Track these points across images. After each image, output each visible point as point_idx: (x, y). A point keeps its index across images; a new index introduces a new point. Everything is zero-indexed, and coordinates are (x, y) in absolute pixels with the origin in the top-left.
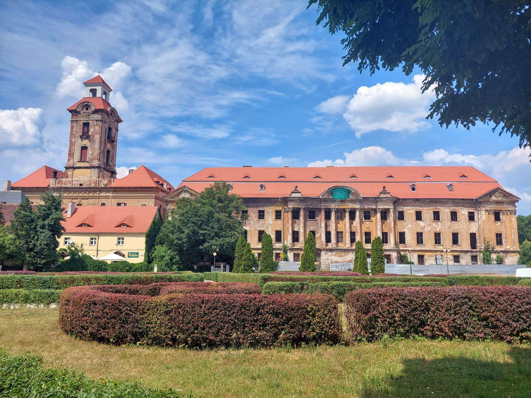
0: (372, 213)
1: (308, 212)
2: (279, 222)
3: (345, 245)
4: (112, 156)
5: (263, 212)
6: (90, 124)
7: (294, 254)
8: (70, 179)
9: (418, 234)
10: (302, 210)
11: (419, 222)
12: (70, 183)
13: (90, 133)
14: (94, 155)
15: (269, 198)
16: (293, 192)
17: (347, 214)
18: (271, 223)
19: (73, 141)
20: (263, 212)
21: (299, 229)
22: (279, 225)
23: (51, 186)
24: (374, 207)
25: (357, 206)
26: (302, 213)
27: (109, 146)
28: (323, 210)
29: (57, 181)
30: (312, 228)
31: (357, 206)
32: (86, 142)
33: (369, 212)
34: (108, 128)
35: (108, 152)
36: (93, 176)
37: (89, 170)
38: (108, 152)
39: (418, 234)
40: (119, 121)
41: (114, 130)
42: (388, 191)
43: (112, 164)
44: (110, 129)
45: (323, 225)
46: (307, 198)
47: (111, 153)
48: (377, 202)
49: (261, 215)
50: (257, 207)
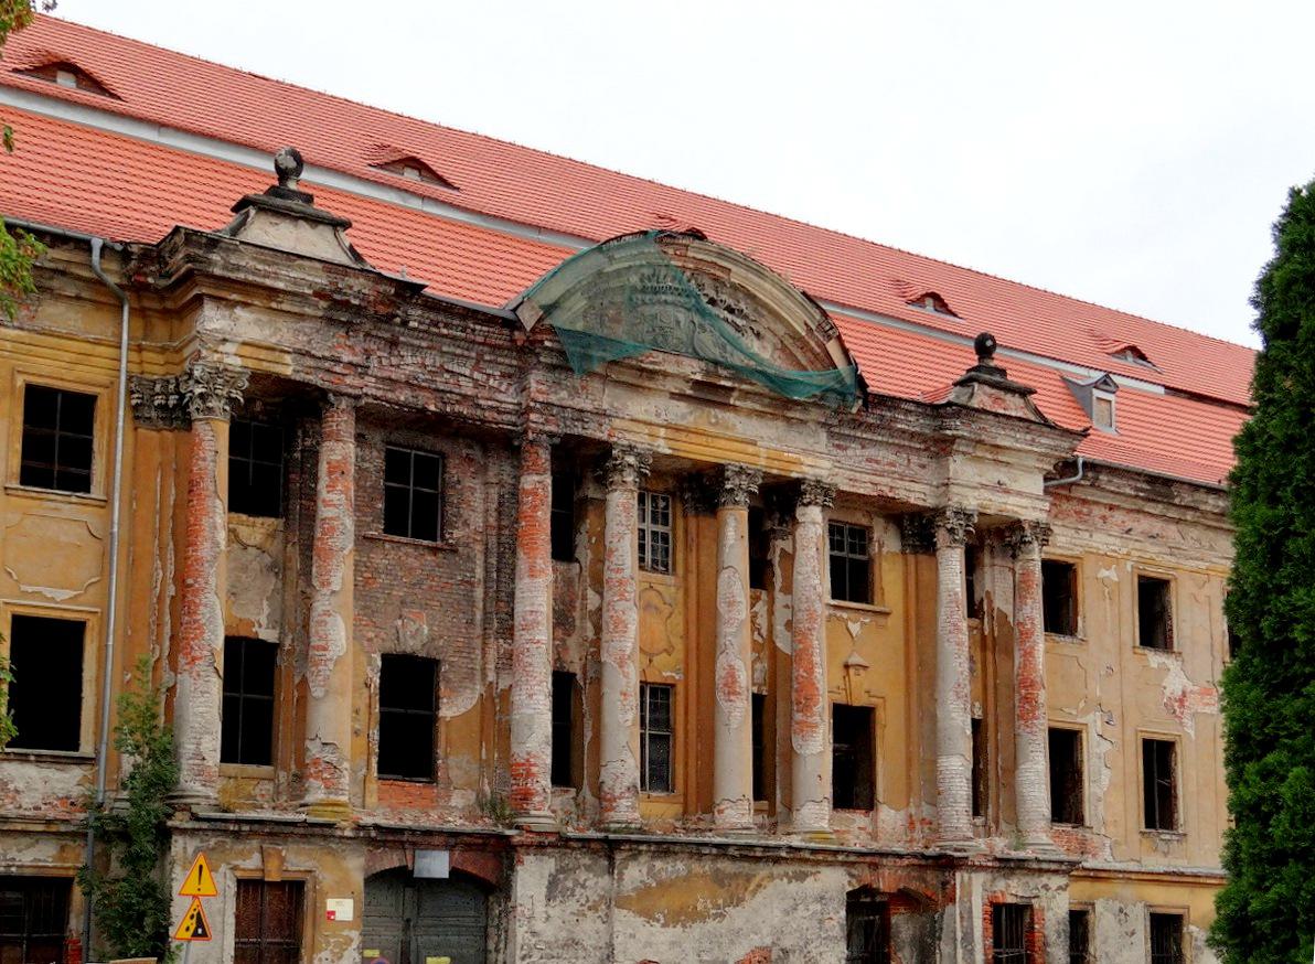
0: (886, 543)
2: (59, 513)
3: (704, 799)
7: (249, 888)
9: (1148, 745)
10: (341, 422)
11: (1155, 659)
17: (735, 527)
24: (917, 494)
25: (811, 456)
28: (544, 456)
30: (416, 634)
31: (811, 456)
33: (861, 536)
39: (1148, 745)
42: (1014, 378)
45: (536, 592)
46: (409, 292)
48: (941, 447)
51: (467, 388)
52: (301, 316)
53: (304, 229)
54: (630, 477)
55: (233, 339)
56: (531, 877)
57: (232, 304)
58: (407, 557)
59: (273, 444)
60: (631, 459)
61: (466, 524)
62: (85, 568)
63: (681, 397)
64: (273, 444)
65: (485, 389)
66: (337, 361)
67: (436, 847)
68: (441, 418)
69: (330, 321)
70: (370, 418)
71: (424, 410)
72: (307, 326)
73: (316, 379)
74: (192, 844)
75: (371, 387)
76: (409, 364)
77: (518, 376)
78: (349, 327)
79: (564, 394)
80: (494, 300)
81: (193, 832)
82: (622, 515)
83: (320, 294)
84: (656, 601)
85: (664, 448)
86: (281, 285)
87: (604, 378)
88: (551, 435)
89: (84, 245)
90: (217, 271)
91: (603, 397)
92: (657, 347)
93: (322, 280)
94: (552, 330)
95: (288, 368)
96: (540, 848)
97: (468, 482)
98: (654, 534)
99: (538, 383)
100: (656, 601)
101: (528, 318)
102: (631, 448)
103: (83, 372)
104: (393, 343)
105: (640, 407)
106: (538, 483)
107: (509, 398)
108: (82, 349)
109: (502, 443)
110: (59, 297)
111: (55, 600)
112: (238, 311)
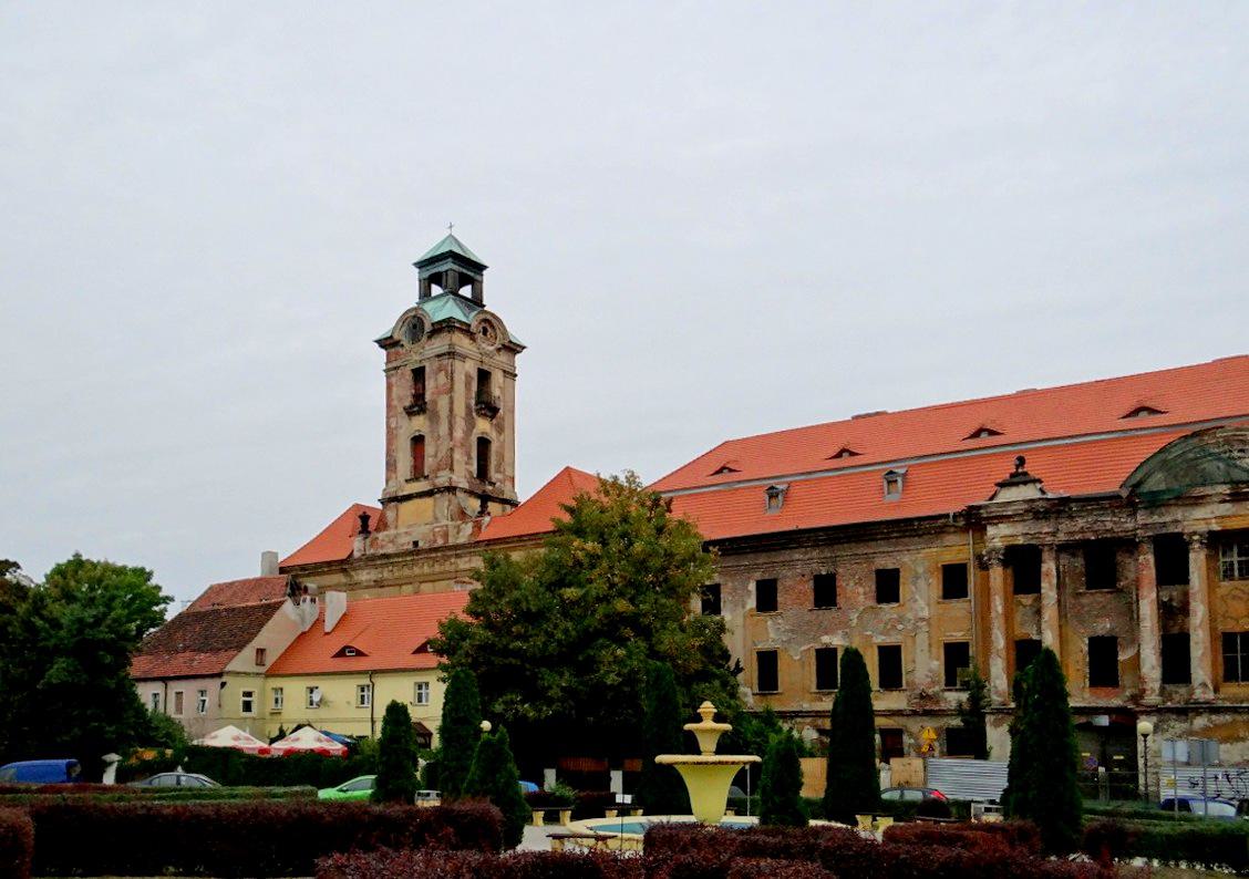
1: (1079, 562)
2: (958, 607)
4: (501, 457)
5: (896, 572)
6: (427, 369)
8: (392, 532)
10: (1046, 555)
12: (392, 542)
13: (428, 397)
14: (440, 456)
15: (909, 521)
16: (1002, 485)
18: (925, 614)
19: (393, 426)
20: (896, 572)
21: (1040, 632)
22: (957, 621)
23: (357, 554)
26: (1049, 566)
27: (483, 426)
29: (368, 540)
32: (420, 424)
34: (475, 375)
35: (484, 444)
36: (439, 515)
37: (429, 501)
38: (484, 444)
40: (513, 349)
41: (497, 378)
43: (499, 476)
44: (484, 376)
47: (494, 447)
49: (888, 587)
50: (868, 558)
51: (1109, 525)
52: (1024, 521)
53: (1022, 488)
54: (1197, 546)
55: (998, 536)
56: (1144, 725)
57: (996, 524)
58: (1101, 597)
59: (1023, 566)
60: (1196, 537)
61: (1127, 578)
62: (966, 625)
63: (1224, 501)
64: (1023, 566)
65: (1124, 524)
66: (1041, 533)
67: (1100, 714)
68: (1097, 540)
69: (1038, 519)
70: (1063, 548)
71: (1089, 540)
72: (1027, 523)
73: (1033, 542)
74: (993, 718)
75: (1062, 537)
76: (1081, 523)
77: (1133, 514)
78: (1047, 519)
79: (1156, 517)
80: (1112, 487)
81: (992, 713)
82: (1197, 560)
83: (1026, 511)
84: (1241, 595)
85: (1216, 527)
86: (1010, 513)
87: (1176, 505)
88: (1149, 537)
89: (947, 516)
90: (985, 515)
91: (1179, 514)
92: (1203, 485)
93: (1026, 506)
94: (1138, 496)
95: (1021, 541)
96: (1148, 713)
97: (1128, 560)
98: (1239, 562)
99: (1142, 518)
100: (1241, 595)
101: (1125, 493)
102: (1195, 533)
103: (961, 556)
104: (1071, 518)
105: (1200, 513)
106: (1147, 559)
107: (1130, 526)
108: (957, 549)
109: (1130, 545)
110: (949, 533)
111: (958, 636)
112: (1000, 525)
